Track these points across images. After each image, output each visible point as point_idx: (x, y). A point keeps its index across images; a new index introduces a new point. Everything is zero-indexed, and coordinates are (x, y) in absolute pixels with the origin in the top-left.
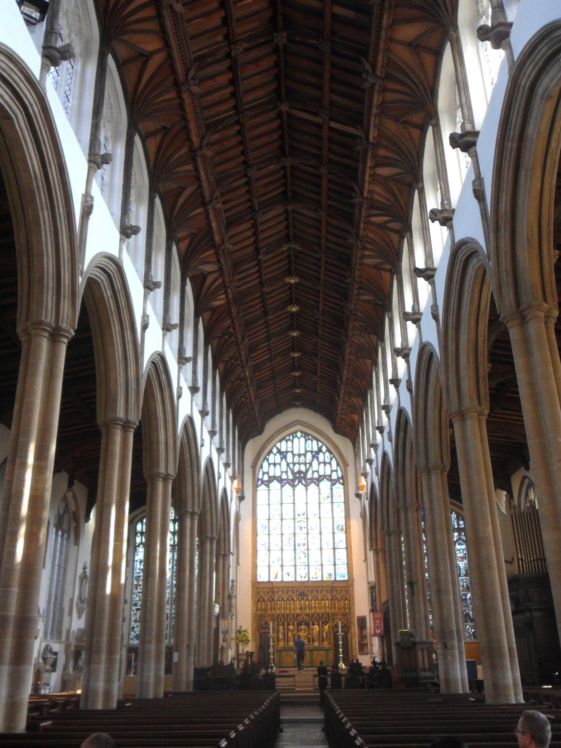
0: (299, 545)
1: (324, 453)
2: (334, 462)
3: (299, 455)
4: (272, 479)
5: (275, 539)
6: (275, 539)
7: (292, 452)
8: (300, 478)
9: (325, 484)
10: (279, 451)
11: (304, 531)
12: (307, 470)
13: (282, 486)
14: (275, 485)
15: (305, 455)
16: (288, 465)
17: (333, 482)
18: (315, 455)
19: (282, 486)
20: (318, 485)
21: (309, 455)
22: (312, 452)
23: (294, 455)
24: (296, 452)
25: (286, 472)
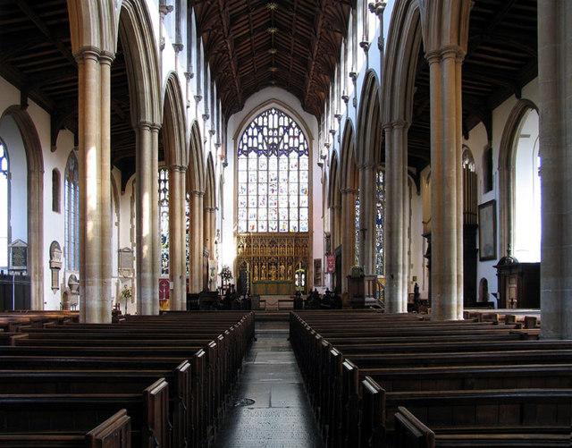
0: (271, 204)
1: (294, 129)
2: (302, 137)
3: (273, 130)
4: (250, 149)
5: (252, 198)
6: (252, 198)
7: (267, 127)
8: (274, 149)
9: (294, 154)
10: (257, 125)
11: (275, 193)
12: (279, 143)
13: (259, 156)
14: (253, 154)
15: (278, 130)
16: (264, 138)
17: (300, 154)
18: (287, 130)
19: (259, 156)
20: (288, 156)
21: (281, 130)
22: (283, 127)
23: (269, 130)
24: (271, 126)
25: (262, 144)
